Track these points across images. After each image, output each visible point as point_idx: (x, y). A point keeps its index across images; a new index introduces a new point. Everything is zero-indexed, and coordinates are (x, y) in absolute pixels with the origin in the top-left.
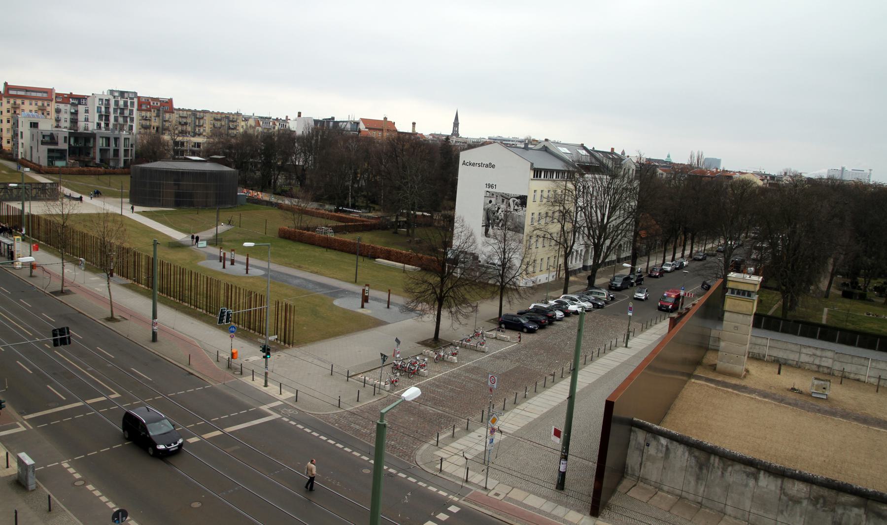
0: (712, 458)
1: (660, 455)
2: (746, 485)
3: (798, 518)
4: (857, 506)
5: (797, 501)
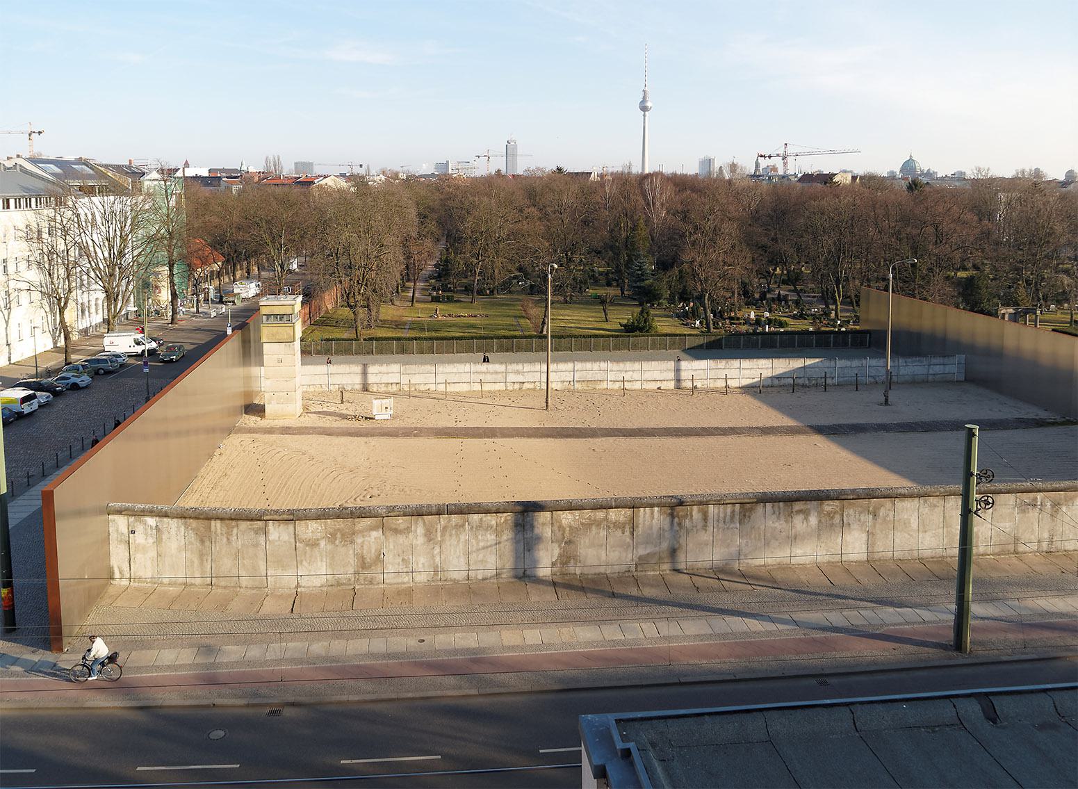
0: (213, 522)
1: (151, 540)
2: (256, 545)
3: (319, 563)
5: (313, 544)
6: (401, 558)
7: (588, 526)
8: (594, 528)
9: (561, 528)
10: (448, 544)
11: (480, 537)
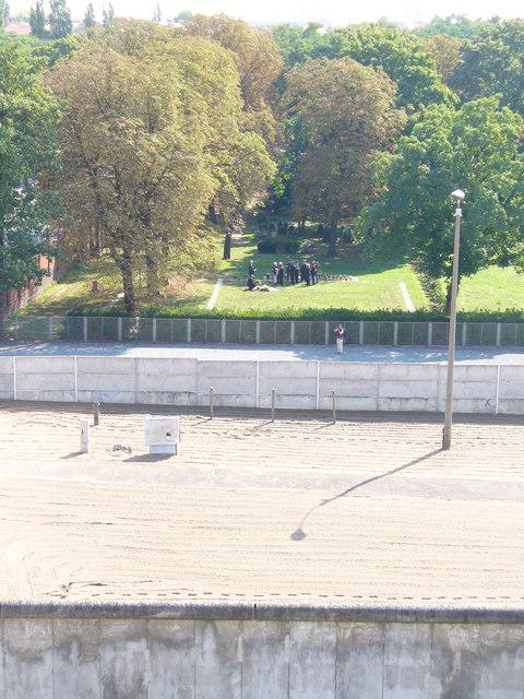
4: (132, 637)
6: (177, 686)
7: (496, 652)
8: (504, 656)
9: (447, 652)
10: (255, 668)
11: (309, 661)
